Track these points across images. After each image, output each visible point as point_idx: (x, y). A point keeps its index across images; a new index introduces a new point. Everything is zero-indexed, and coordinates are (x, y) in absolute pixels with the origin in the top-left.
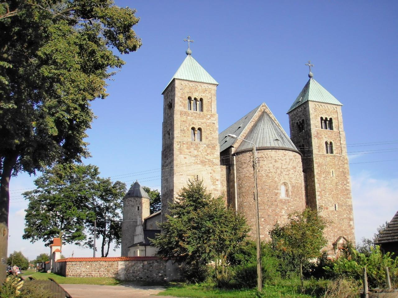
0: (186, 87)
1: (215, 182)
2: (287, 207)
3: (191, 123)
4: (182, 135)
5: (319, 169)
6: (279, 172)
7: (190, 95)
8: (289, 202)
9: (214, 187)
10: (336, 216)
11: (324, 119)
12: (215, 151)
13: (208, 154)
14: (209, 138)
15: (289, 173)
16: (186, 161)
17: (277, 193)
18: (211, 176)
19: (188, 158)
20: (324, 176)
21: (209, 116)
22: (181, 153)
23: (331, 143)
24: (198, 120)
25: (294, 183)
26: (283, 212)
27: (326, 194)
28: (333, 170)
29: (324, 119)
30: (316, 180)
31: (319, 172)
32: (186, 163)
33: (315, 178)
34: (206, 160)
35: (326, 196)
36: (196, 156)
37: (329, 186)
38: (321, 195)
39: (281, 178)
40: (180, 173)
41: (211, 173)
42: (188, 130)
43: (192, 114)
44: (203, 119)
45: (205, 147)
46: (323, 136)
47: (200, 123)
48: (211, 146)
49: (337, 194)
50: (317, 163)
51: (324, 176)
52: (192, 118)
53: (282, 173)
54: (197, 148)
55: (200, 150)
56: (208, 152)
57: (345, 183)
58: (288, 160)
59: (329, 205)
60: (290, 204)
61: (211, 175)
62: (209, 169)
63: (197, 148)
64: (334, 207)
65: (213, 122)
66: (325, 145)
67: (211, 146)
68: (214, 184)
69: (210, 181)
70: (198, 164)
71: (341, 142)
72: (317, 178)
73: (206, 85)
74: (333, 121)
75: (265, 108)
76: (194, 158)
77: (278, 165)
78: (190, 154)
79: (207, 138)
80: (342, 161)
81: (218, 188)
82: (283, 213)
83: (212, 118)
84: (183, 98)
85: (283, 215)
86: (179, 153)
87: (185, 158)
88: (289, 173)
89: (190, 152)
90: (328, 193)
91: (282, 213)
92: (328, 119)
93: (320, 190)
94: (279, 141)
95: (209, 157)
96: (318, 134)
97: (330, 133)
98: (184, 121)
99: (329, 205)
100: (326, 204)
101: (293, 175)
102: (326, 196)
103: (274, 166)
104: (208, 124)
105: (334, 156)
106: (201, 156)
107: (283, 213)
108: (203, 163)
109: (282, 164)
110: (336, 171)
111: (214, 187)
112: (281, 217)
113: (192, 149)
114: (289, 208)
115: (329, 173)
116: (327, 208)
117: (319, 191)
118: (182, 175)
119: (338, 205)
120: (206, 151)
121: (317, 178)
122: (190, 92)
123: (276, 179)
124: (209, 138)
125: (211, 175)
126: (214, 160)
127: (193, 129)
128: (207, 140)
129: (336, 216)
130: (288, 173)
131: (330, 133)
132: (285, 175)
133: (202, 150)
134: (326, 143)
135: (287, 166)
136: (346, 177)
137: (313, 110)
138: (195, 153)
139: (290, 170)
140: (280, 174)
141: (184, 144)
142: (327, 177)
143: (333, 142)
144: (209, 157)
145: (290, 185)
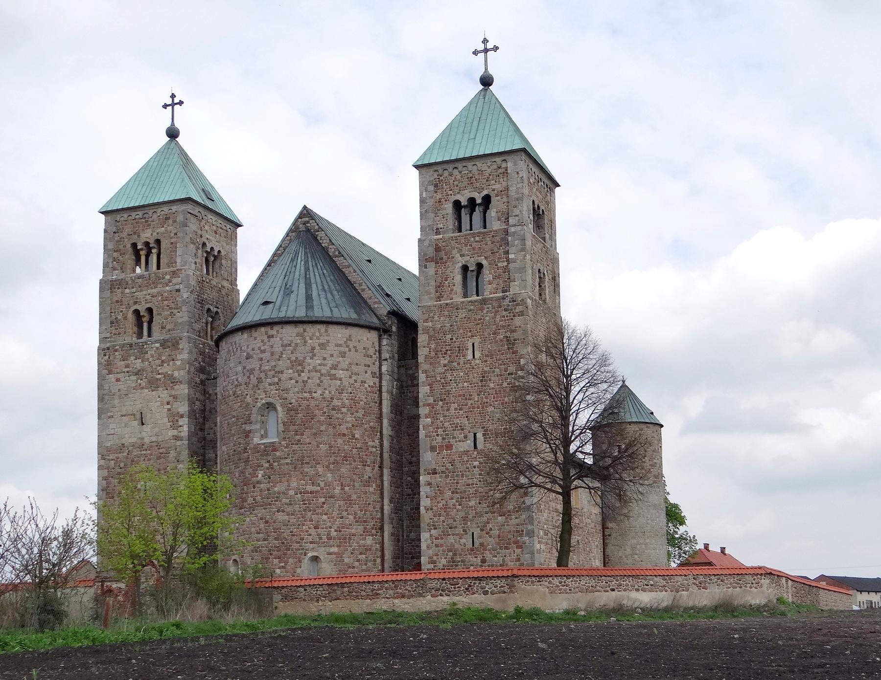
0: (126, 224)
1: (177, 421)
2: (269, 462)
3: (131, 302)
4: (114, 331)
5: (433, 346)
6: (254, 380)
7: (134, 239)
8: (275, 450)
9: (175, 432)
10: (476, 463)
11: (464, 202)
12: (177, 352)
13: (163, 362)
14: (168, 327)
15: (280, 380)
16: (121, 386)
17: (250, 431)
18: (169, 410)
19: (122, 379)
20: (446, 362)
21: (168, 277)
22: (110, 372)
23: (480, 266)
24: (145, 292)
25: (293, 401)
26: (260, 474)
27: (448, 410)
28: (477, 340)
29: (464, 202)
30: (422, 377)
31: (433, 354)
32: (119, 390)
33: (420, 372)
34: (159, 377)
35: (447, 413)
36: (139, 371)
37: (460, 385)
38: (434, 415)
39: (259, 395)
40: (109, 414)
41: (168, 403)
42: (125, 318)
43: (133, 281)
44: (156, 287)
45: (157, 348)
46: (455, 252)
47: (148, 297)
48: (170, 344)
49: (484, 405)
50: (426, 331)
51: (446, 362)
52: (134, 290)
53: (260, 380)
54: (142, 353)
55: (148, 356)
56: (164, 358)
57: (512, 368)
58: (278, 349)
59: (454, 438)
60: (278, 454)
61: (169, 407)
62: (164, 394)
63: (142, 353)
64: (470, 442)
65: (177, 287)
66: (458, 278)
67: (170, 344)
68: (175, 425)
69: (166, 420)
70: (143, 388)
71: (511, 256)
72: (425, 372)
73: (165, 209)
74: (494, 199)
75: (307, 219)
76: (134, 378)
77: (254, 364)
78: (128, 369)
79: (163, 328)
80: (506, 310)
81: (182, 434)
82: (260, 476)
83: (175, 281)
84: (120, 251)
85: (259, 482)
86: (106, 371)
87: (118, 380)
88: (280, 380)
89: (127, 366)
90: (452, 408)
91: (257, 476)
92: (479, 201)
93: (431, 400)
94: (271, 306)
95: (166, 369)
96: (438, 249)
97: (477, 239)
98: (117, 302)
99: (454, 438)
100: (447, 435)
101: (293, 381)
102: (447, 413)
103: (244, 368)
104: (166, 294)
105: (484, 301)
106: (149, 369)
107: (260, 476)
108: (153, 385)
109: (261, 359)
110: (484, 340)
111: (175, 432)
112: (254, 487)
113: (133, 358)
114: (276, 464)
115: (461, 350)
116: (449, 447)
117: (429, 405)
118: (112, 417)
119: (484, 435)
120: (160, 355)
121: (425, 372)
122: (135, 233)
123: (249, 399)
124: (168, 327)
125: (169, 407)
126: (176, 374)
127: (137, 312)
128: (164, 331)
129: (476, 463)
130: (276, 380)
131: (477, 239)
132: (270, 384)
133: (152, 356)
134: (465, 268)
135: (274, 363)
136: (515, 352)
137: (431, 188)
138: (138, 364)
139: (282, 372)
140: (257, 386)
141: (116, 351)
142: (455, 364)
143: (484, 262)
144: (166, 369)
145: (279, 408)
